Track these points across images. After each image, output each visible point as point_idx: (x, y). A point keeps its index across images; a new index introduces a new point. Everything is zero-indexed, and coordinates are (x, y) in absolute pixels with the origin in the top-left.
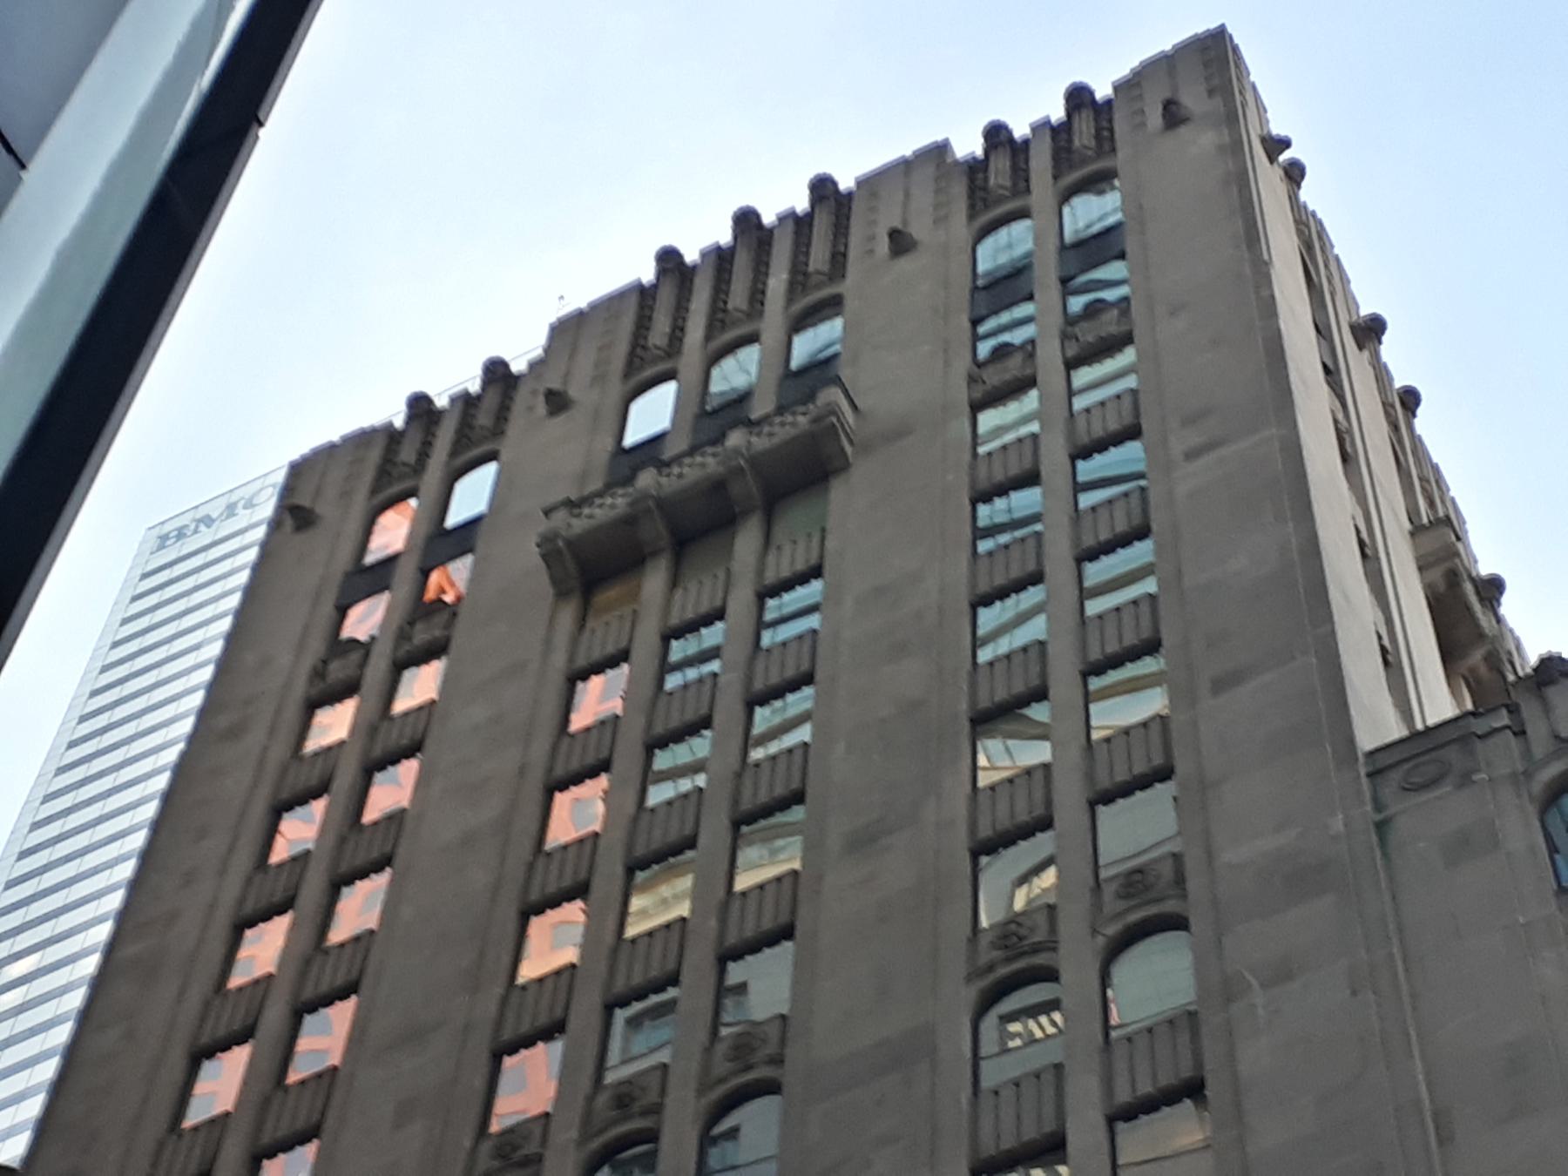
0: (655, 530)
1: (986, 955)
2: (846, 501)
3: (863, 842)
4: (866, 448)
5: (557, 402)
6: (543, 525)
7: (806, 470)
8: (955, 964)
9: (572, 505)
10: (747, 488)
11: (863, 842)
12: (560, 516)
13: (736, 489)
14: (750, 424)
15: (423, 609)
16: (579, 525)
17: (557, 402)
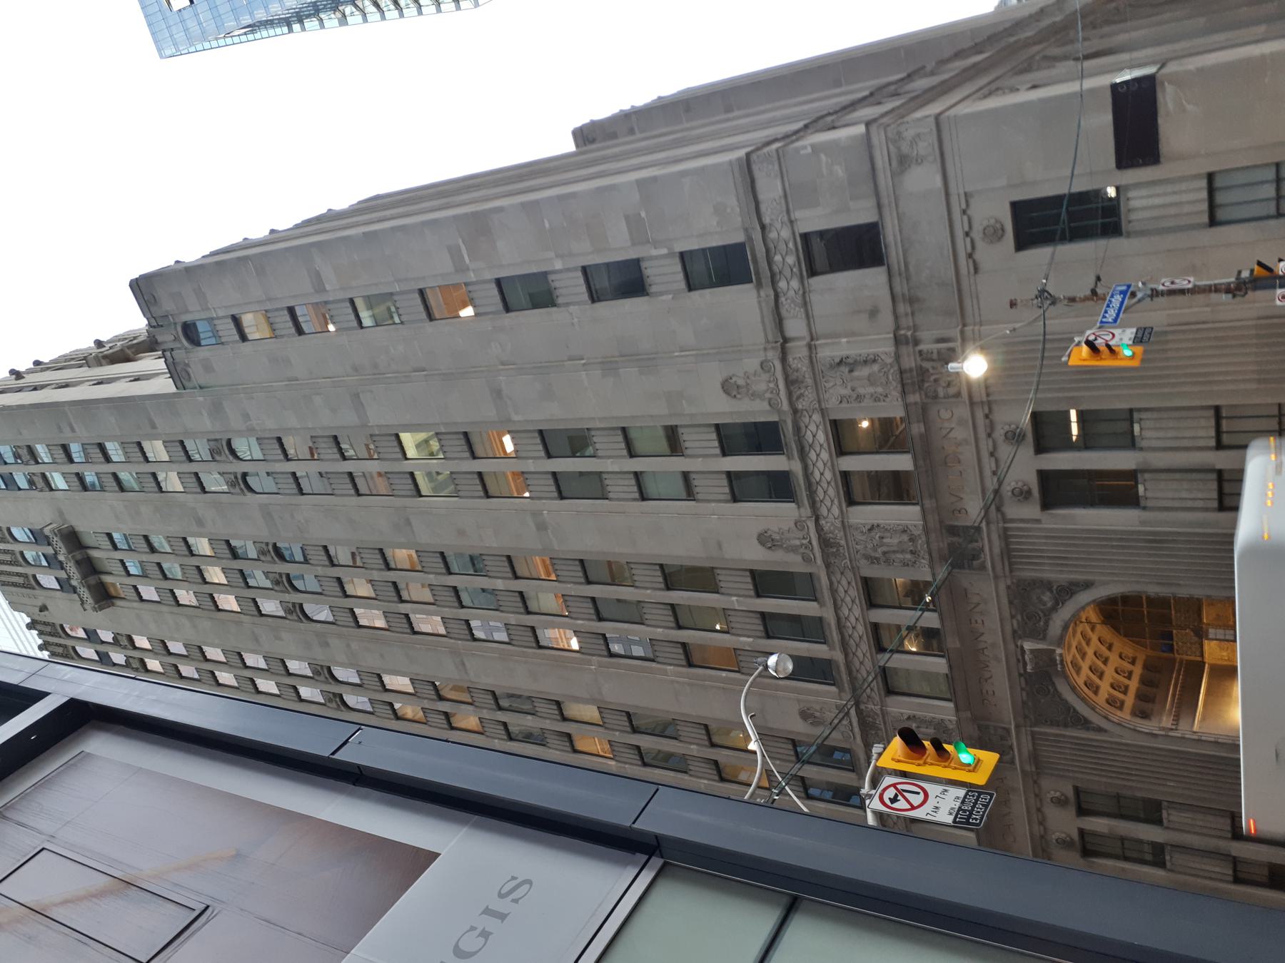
0: (92, 580)
1: (237, 490)
2: (82, 526)
3: (200, 523)
4: (65, 521)
5: (43, 608)
6: (90, 611)
7: (72, 539)
8: (241, 498)
9: (83, 603)
10: (78, 555)
11: (200, 523)
12: (86, 606)
13: (79, 557)
14: (56, 553)
15: (116, 642)
16: (90, 601)
17: (43, 608)
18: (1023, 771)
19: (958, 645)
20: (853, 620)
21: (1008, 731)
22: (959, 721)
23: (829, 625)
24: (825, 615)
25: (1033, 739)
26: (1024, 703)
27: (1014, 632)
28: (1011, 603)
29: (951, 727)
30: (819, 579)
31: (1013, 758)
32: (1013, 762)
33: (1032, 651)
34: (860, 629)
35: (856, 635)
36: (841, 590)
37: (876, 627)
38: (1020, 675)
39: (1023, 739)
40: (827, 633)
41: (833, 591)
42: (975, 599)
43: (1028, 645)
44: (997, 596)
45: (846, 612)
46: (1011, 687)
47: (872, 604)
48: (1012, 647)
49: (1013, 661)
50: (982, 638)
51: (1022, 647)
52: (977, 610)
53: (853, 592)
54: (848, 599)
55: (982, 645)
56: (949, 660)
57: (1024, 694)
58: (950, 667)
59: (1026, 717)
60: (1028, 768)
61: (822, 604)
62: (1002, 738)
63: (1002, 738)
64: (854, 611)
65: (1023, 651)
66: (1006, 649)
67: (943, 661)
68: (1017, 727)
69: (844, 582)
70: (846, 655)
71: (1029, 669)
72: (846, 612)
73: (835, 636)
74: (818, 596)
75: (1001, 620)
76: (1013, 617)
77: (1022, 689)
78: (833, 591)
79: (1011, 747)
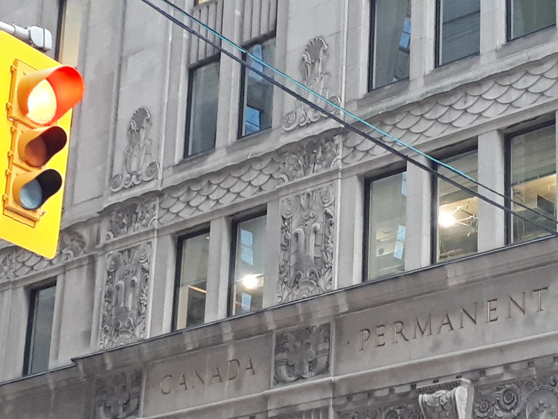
18: (266, 398)
19: (452, 283)
20: (477, 109)
21: (325, 371)
22: (332, 294)
23: (467, 68)
24: (483, 60)
25: (317, 410)
26: (370, 394)
27: (482, 371)
28: (530, 362)
29: (322, 282)
30: (546, 41)
31: (285, 382)
32: (279, 381)
33: (452, 401)
34: (464, 123)
35: (454, 115)
36: (529, 81)
37: (470, 147)
38: (413, 385)
39: (316, 396)
40: (453, 68)
41: (526, 68)
42: (531, 306)
43: (462, 395)
44: (539, 340)
45: (490, 96)
46: (393, 372)
47: (508, 138)
48: (457, 369)
49: (435, 373)
50: (467, 322)
51: (457, 384)
52: (515, 309)
53: (526, 103)
54: (514, 95)
55: (455, 323)
56: (426, 270)
57: (386, 392)
58: (415, 274)
59: (349, 397)
60: (272, 405)
61: (501, 53)
62: (313, 364)
63: (313, 364)
64: (492, 109)
65: (450, 386)
66: (451, 360)
67: (425, 262)
68: (333, 385)
69: (543, 85)
70: (418, 104)
71: (425, 397)
72: (490, 96)
73: (448, 82)
74: (515, 45)
75: (501, 349)
76: (507, 367)
77: (391, 390)
78: (526, 68)
79: (300, 378)
